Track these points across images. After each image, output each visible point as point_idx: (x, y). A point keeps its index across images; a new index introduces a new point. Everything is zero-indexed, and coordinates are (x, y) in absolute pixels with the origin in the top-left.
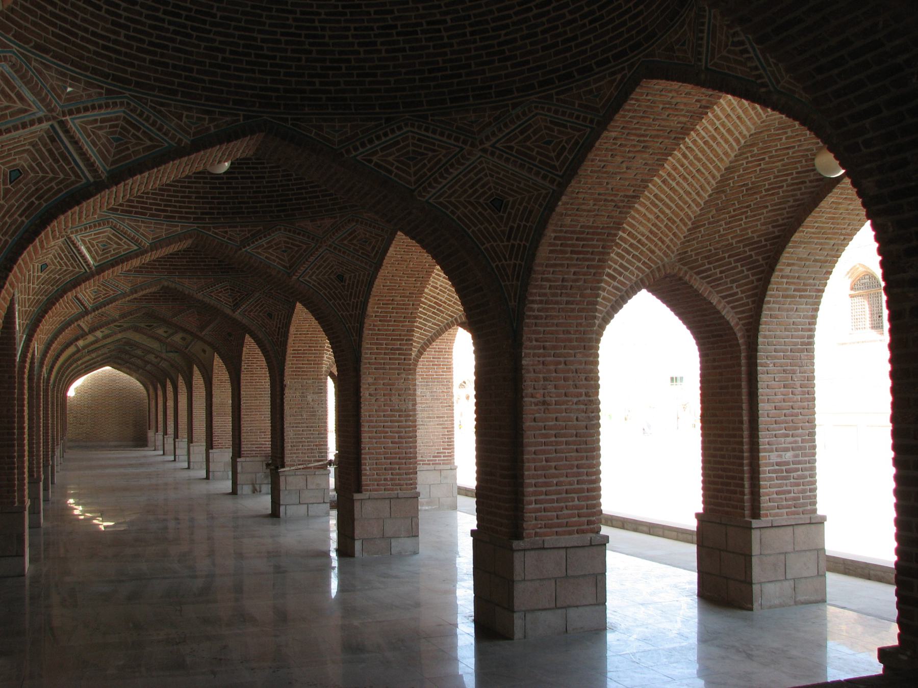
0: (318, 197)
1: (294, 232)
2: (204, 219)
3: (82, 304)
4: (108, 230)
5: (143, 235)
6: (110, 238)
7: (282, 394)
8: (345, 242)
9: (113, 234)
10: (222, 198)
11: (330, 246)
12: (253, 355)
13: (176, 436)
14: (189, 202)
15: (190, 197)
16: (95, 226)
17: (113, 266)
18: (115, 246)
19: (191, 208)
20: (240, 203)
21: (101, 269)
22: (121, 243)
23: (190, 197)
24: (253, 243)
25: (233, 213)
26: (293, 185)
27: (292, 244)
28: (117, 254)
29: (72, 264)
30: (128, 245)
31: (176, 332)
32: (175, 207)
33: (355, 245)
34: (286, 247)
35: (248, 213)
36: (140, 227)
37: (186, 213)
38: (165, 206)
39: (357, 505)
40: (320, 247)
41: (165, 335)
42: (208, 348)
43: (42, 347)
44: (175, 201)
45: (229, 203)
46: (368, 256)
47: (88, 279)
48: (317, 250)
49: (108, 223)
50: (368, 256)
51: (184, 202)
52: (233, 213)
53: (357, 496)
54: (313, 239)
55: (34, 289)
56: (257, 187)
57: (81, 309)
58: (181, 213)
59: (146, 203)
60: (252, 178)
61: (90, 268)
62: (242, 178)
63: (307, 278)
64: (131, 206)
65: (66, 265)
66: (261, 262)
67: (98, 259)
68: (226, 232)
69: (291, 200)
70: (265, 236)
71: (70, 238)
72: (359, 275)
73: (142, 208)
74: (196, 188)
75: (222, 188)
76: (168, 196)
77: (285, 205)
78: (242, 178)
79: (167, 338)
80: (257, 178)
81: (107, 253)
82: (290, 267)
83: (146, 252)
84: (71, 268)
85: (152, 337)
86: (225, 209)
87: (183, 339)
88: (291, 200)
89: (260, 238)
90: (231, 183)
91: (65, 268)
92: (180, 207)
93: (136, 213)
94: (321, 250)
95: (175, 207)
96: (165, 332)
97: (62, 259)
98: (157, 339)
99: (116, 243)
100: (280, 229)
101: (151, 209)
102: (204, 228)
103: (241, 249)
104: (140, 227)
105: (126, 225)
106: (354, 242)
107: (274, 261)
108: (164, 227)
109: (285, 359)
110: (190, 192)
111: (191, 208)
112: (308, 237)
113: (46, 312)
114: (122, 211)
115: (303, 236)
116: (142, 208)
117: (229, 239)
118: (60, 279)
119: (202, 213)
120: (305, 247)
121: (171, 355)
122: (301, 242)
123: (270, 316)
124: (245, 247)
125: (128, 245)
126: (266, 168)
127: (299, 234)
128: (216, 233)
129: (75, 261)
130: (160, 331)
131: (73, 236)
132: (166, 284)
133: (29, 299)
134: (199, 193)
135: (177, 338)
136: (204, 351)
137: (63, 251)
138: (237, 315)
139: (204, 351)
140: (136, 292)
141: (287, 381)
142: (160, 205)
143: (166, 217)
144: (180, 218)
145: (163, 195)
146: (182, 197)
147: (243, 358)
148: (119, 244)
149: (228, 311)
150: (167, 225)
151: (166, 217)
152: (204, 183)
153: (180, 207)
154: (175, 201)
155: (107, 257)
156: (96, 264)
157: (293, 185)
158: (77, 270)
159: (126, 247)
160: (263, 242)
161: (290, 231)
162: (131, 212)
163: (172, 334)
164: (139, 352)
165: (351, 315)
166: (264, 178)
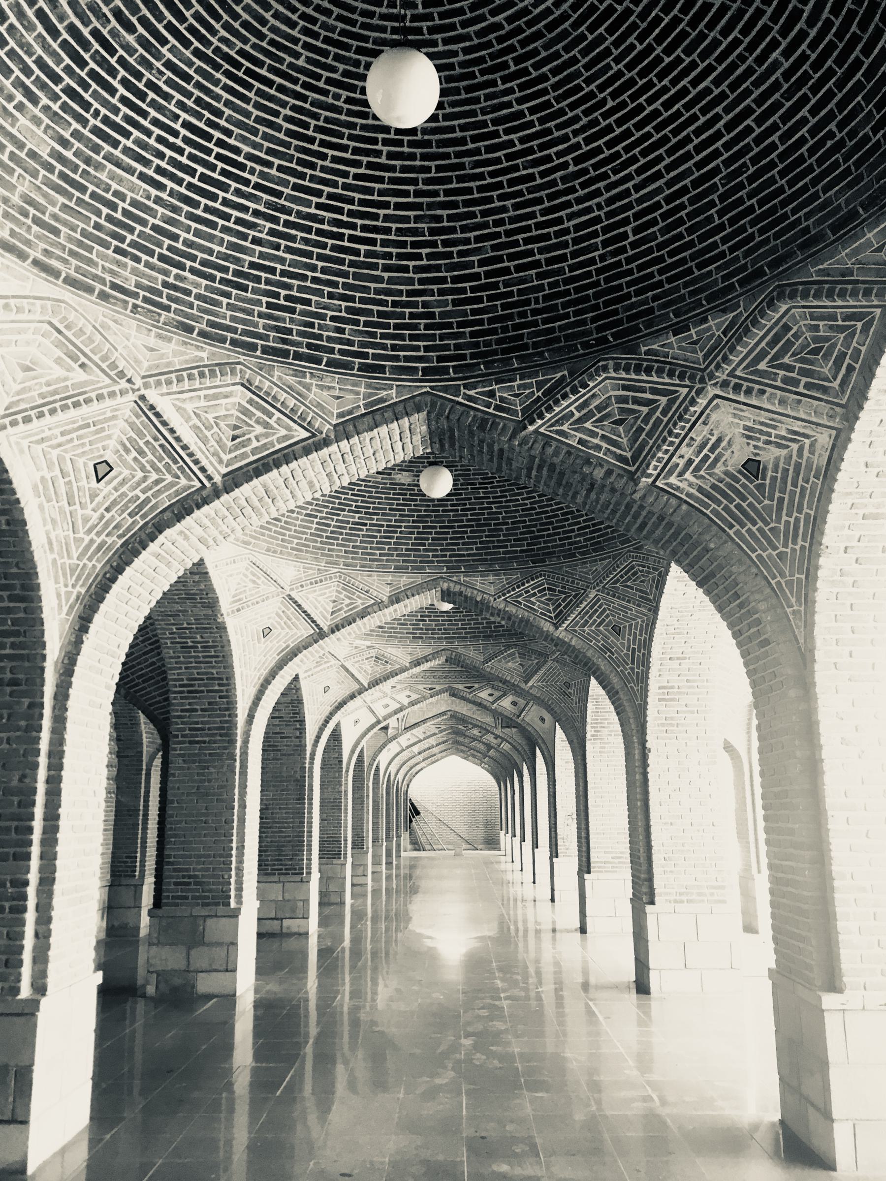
0: (689, 271)
1: (638, 369)
2: (445, 370)
3: (314, 622)
4: (241, 396)
5: (318, 405)
6: (245, 412)
7: (645, 765)
8: (762, 366)
9: (250, 402)
10: (480, 322)
11: (725, 384)
12: (599, 705)
13: (523, 839)
14: (412, 338)
15: (415, 327)
16: (202, 375)
17: (258, 473)
18: (259, 429)
19: (417, 348)
20: (516, 327)
21: (235, 479)
22: (272, 422)
23: (415, 327)
24: (549, 409)
25: (504, 351)
26: (629, 260)
27: (636, 401)
28: (265, 447)
29: (168, 467)
30: (289, 429)
31: (504, 695)
32: (384, 347)
33: (789, 368)
34: (622, 411)
35: (535, 345)
36: (308, 387)
37: (407, 359)
38: (362, 345)
39: (832, 1026)
40: (699, 392)
41: (491, 699)
42: (547, 717)
43: (252, 691)
44: (383, 336)
45: (494, 332)
46: (825, 390)
47: (206, 501)
48: (693, 402)
49: (233, 372)
50: (825, 390)
51: (402, 337)
52: (504, 351)
53: (829, 1000)
54: (682, 377)
55: (86, 520)
56: (551, 285)
57: (306, 630)
58: (397, 358)
59: (319, 337)
60: (537, 264)
61: (210, 478)
62: (519, 268)
63: (673, 480)
64: (284, 341)
65: (157, 470)
66: (569, 453)
67: (225, 458)
68: (491, 394)
69: (628, 296)
70: (574, 391)
71: (143, 398)
72: (800, 451)
73: (309, 346)
74: (425, 305)
75: (479, 300)
76: (366, 324)
77: (615, 312)
78: (519, 268)
79: (493, 703)
80: (549, 261)
81: (243, 445)
82: (635, 458)
83: (326, 443)
84: (169, 478)
85: (474, 703)
86: (487, 344)
87: (514, 703)
88: (628, 296)
89: (565, 396)
90: (495, 286)
91: (154, 476)
92: (394, 348)
93: (298, 356)
94: (702, 401)
95: (384, 347)
96: (491, 695)
97: (141, 453)
98: (480, 705)
99: (258, 422)
100: (605, 369)
101: (331, 351)
102: (445, 389)
103: (525, 428)
104: (308, 387)
105: (278, 377)
106: (786, 360)
107: (598, 448)
108: (363, 390)
109: (646, 703)
110: (412, 316)
111: (417, 348)
112: (671, 374)
113: (120, 570)
114: (266, 350)
115: (660, 372)
116: (309, 346)
117: (497, 408)
118: (147, 500)
119: (440, 359)
120: (664, 400)
121: (507, 730)
122: (654, 391)
123: (617, 630)
124: (532, 422)
125: (289, 429)
126: (566, 231)
127: (648, 371)
128: (470, 398)
129: (175, 462)
130: (484, 695)
131: (153, 396)
132: (445, 586)
133: (78, 541)
134: (431, 315)
135: (506, 703)
136: (543, 720)
137: (141, 435)
138: (561, 633)
139: (543, 720)
140: (398, 601)
141: (652, 741)
142: (350, 343)
143: (364, 368)
144: (394, 369)
145: (356, 323)
146: (397, 326)
147: (588, 720)
148: (266, 425)
149: (547, 627)
150: (368, 386)
151: (364, 368)
152: (441, 292)
153: (394, 348)
154: (383, 336)
155: (244, 456)
156: (224, 470)
157: (629, 260)
158: (183, 481)
159: (283, 432)
160: (569, 404)
161: (627, 370)
162: (285, 354)
163: (499, 698)
164: (476, 732)
165: (781, 556)
166: (563, 258)
